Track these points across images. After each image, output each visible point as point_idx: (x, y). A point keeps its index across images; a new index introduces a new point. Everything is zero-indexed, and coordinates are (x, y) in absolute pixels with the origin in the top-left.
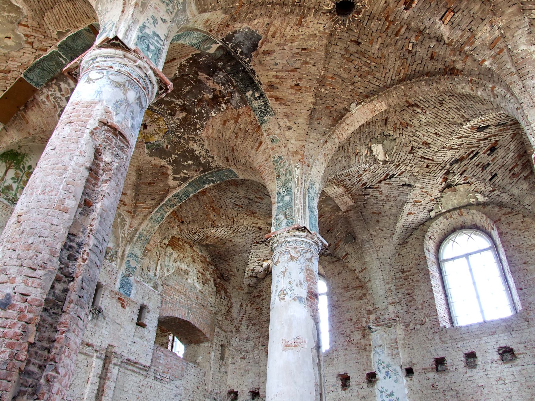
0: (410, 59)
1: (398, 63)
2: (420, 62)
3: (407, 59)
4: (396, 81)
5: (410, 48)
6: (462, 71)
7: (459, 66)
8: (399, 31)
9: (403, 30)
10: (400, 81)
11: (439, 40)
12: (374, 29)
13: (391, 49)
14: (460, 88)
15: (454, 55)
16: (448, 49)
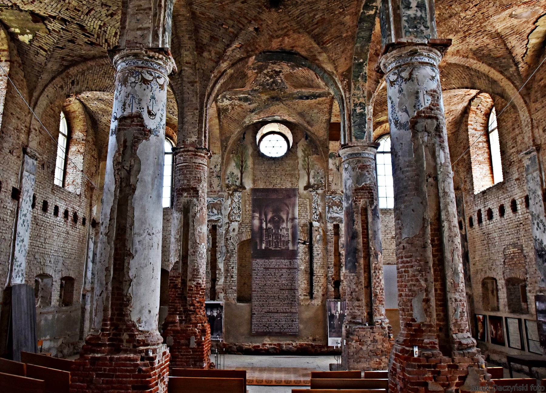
0: (214, 24)
1: (212, 16)
2: (209, 28)
3: (214, 22)
4: (194, 10)
5: (224, 26)
6: (201, 56)
7: (205, 54)
8: (241, 24)
9: (241, 26)
10: (193, 13)
11: (229, 46)
12: (250, 12)
13: (227, 16)
14: (186, 53)
15: (215, 53)
16: (221, 51)
